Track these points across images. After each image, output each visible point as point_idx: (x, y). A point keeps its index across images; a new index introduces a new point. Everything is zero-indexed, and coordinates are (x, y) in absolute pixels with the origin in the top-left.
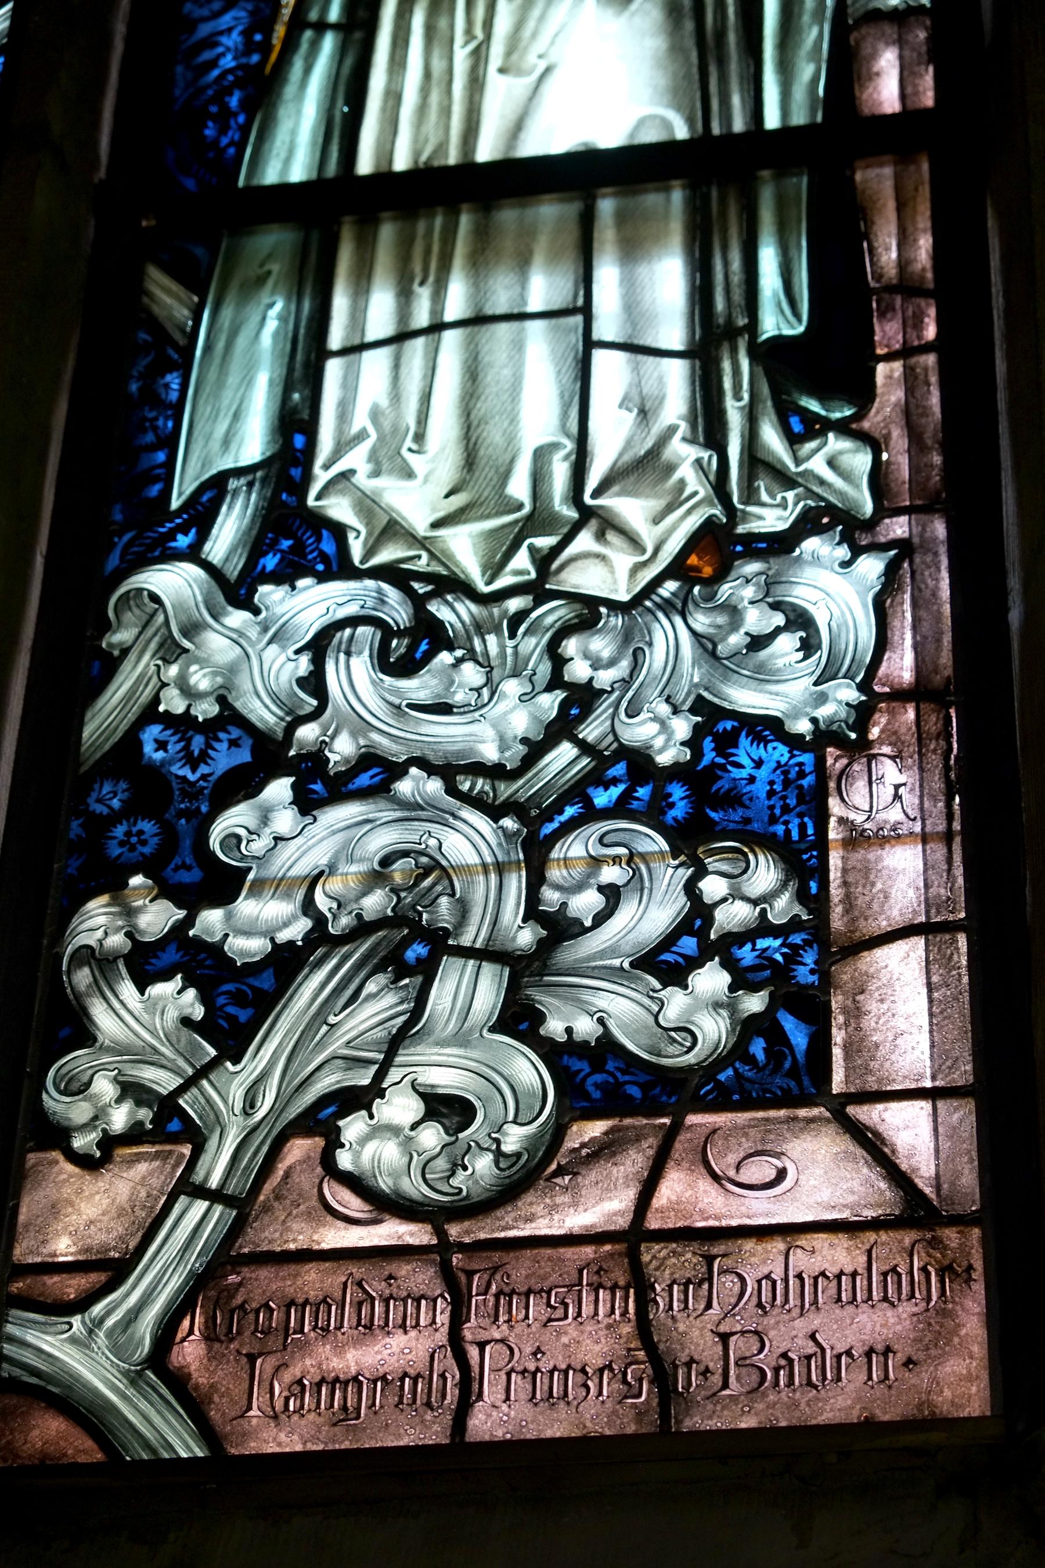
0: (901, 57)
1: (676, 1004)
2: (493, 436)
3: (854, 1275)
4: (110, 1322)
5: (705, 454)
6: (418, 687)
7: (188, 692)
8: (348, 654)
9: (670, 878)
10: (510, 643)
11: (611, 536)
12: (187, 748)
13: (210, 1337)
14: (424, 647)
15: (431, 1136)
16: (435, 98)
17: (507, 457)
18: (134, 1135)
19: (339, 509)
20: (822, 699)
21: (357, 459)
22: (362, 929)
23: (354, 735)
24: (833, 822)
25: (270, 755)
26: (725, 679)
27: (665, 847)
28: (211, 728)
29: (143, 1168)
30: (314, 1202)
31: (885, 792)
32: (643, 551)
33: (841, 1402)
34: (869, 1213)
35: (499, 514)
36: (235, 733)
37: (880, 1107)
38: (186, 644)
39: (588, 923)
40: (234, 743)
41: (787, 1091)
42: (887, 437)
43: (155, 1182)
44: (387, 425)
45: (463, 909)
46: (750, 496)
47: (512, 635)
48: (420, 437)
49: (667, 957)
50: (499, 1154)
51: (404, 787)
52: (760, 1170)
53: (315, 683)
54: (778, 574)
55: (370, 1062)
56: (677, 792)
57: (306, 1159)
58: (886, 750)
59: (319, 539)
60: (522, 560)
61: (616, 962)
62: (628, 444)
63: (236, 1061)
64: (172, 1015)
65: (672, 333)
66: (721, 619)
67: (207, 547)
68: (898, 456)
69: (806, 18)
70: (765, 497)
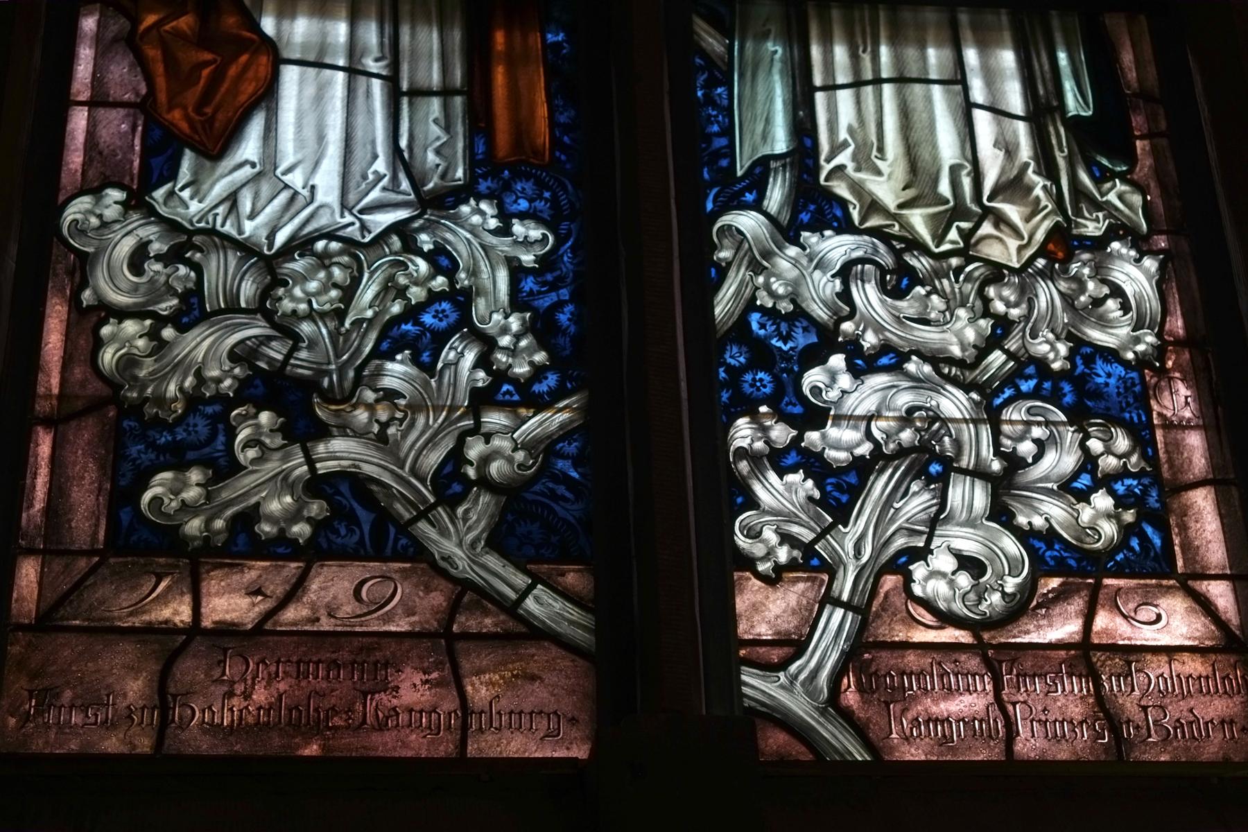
1: (1086, 514)
2: (924, 154)
3: (1207, 678)
4: (802, 677)
5: (1049, 184)
6: (907, 306)
7: (772, 294)
8: (863, 281)
9: (1070, 435)
10: (957, 286)
11: (1002, 227)
12: (778, 329)
13: (860, 689)
14: (905, 282)
15: (964, 580)
17: (935, 170)
18: (792, 565)
19: (842, 190)
20: (1137, 340)
21: (844, 158)
22: (902, 452)
24: (1155, 416)
27: (1064, 418)
28: (791, 318)
30: (905, 614)
31: (1178, 400)
32: (1023, 238)
33: (1213, 749)
34: (1208, 643)
36: (805, 324)
37: (1206, 583)
38: (765, 263)
39: (1030, 460)
40: (805, 330)
41: (1154, 569)
42: (1148, 185)
43: (811, 595)
44: (859, 138)
45: (958, 444)
46: (1078, 213)
47: (957, 281)
48: (881, 149)
50: (1004, 594)
51: (911, 367)
52: (1147, 613)
53: (845, 295)
54: (1100, 262)
55: (921, 533)
56: (1067, 388)
57: (895, 588)
58: (1177, 375)
59: (831, 207)
61: (1050, 485)
62: (1003, 171)
63: (845, 526)
64: (802, 494)
66: (1074, 286)
67: (765, 203)
70: (1087, 214)
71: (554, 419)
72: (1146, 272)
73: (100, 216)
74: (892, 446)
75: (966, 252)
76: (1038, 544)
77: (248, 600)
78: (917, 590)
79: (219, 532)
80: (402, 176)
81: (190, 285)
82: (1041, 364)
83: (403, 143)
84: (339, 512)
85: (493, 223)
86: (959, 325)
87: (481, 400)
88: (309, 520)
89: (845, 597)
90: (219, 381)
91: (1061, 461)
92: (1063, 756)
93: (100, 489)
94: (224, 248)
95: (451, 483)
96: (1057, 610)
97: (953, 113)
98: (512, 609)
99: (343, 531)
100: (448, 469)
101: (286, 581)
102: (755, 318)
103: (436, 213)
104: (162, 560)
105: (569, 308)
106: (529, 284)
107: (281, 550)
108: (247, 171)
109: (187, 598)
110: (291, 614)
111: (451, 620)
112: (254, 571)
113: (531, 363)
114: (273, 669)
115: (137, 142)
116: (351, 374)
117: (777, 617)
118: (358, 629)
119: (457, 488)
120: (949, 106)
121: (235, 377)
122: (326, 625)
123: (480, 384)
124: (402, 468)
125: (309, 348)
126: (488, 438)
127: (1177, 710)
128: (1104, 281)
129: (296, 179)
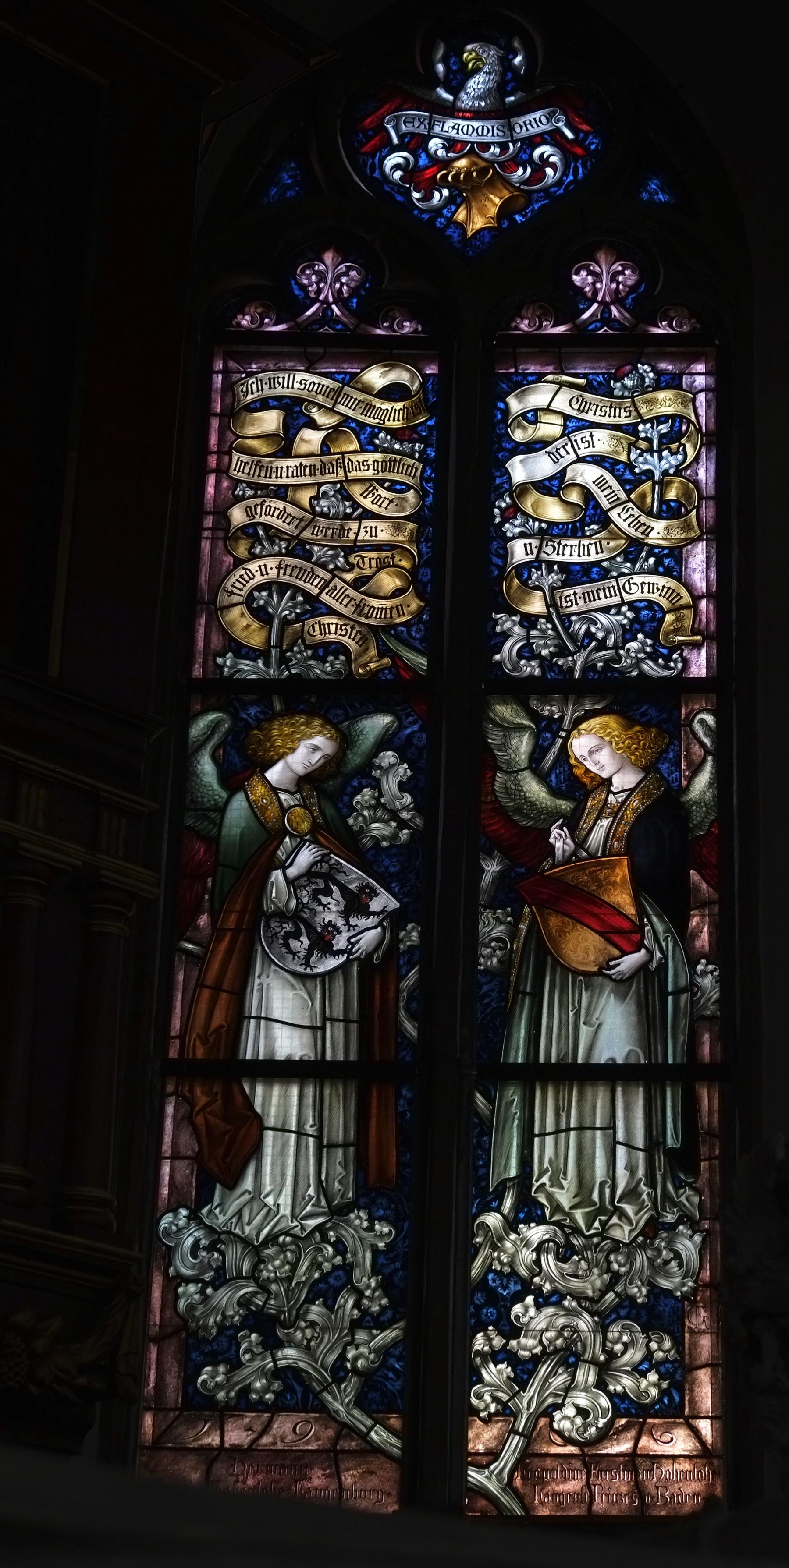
0: (710, 1037)
1: (644, 1384)
2: (587, 1176)
4: (496, 1472)
7: (501, 1263)
8: (547, 1254)
9: (641, 1340)
11: (623, 1219)
12: (502, 1283)
13: (523, 1478)
15: (579, 1421)
16: (563, 1032)
17: (591, 1185)
18: (497, 1413)
19: (542, 1200)
20: (684, 1285)
21: (545, 1179)
22: (556, 1351)
23: (551, 1283)
25: (526, 1287)
26: (657, 1275)
29: (500, 1424)
31: (700, 1319)
32: (632, 1225)
34: (694, 1453)
35: (590, 1206)
36: (516, 1278)
40: (516, 1283)
43: (504, 1429)
44: (554, 1167)
45: (584, 1346)
46: (664, 1210)
48: (565, 1173)
49: (641, 1368)
50: (597, 1427)
51: (566, 1303)
52: (666, 1437)
53: (537, 1262)
55: (560, 1395)
56: (644, 1313)
57: (545, 1425)
60: (597, 1224)
61: (627, 1368)
64: (505, 1375)
65: (639, 1141)
66: (655, 1253)
68: (706, 1197)
69: (681, 1016)
71: (391, 1334)
72: (694, 1243)
73: (177, 1225)
74: (551, 1348)
75: (602, 1234)
76: (617, 1401)
77: (245, 1433)
78: (555, 1426)
79: (232, 1398)
80: (322, 1197)
81: (220, 1263)
82: (632, 1299)
83: (323, 1178)
84: (288, 1387)
85: (365, 1224)
86: (594, 1277)
87: (355, 1325)
88: (274, 1392)
89: (520, 1430)
90: (233, 1317)
91: (635, 1355)
92: (614, 1512)
93: (179, 1376)
94: (236, 1242)
95: (339, 1372)
96: (622, 1436)
97: (605, 1147)
98: (365, 1437)
99: (289, 1397)
100: (338, 1364)
101: (262, 1424)
102: (491, 1276)
103: (338, 1218)
104: (207, 1413)
105: (401, 1273)
106: (381, 1260)
107: (260, 1407)
108: (247, 1197)
109: (218, 1433)
110: (265, 1440)
111: (336, 1443)
112: (249, 1417)
113: (380, 1305)
114: (256, 1468)
115: (194, 1180)
116: (294, 1312)
117: (487, 1441)
118: (294, 1448)
119: (342, 1374)
120: (604, 1144)
121: (240, 1315)
122: (280, 1446)
123: (355, 1317)
124: (317, 1363)
125: (275, 1298)
126: (357, 1347)
127: (674, 1489)
128: (672, 1250)
129: (270, 1200)
